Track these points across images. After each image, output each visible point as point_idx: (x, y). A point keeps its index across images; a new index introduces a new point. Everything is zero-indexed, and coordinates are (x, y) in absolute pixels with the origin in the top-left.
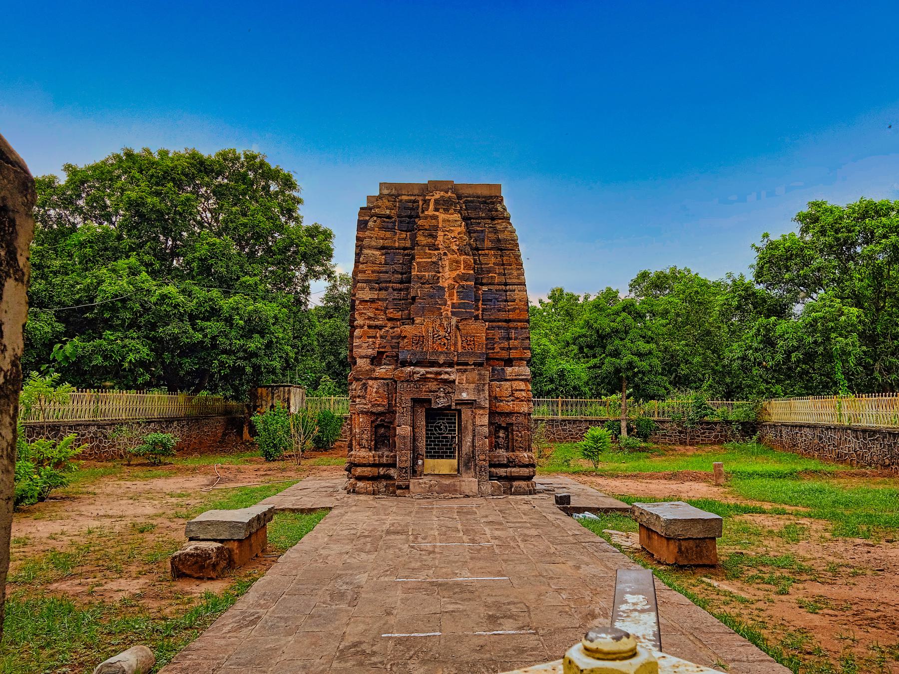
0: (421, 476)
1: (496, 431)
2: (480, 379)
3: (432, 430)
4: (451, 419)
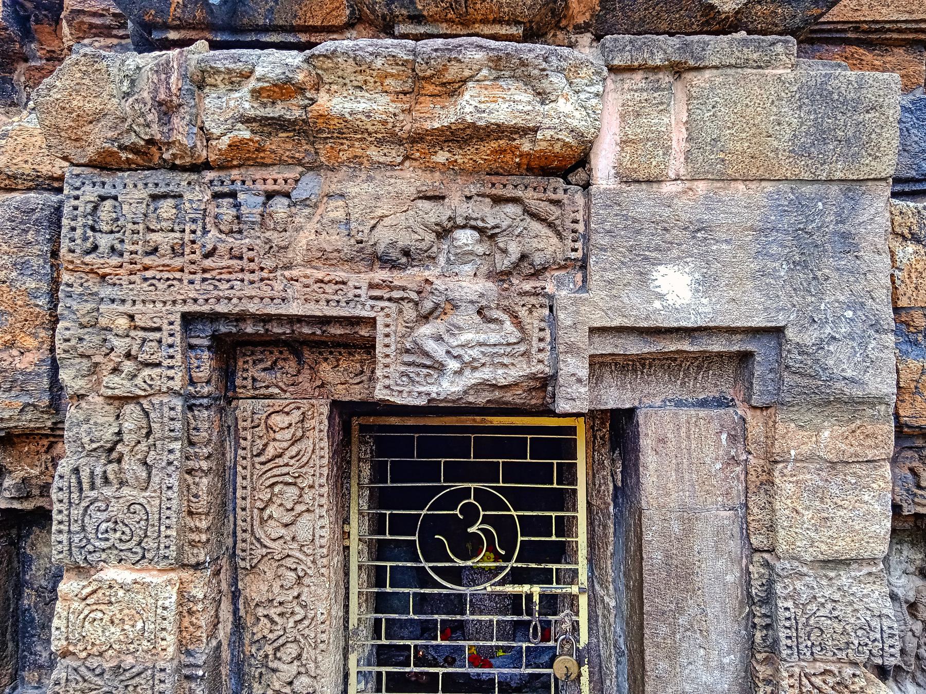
2: (822, 136)
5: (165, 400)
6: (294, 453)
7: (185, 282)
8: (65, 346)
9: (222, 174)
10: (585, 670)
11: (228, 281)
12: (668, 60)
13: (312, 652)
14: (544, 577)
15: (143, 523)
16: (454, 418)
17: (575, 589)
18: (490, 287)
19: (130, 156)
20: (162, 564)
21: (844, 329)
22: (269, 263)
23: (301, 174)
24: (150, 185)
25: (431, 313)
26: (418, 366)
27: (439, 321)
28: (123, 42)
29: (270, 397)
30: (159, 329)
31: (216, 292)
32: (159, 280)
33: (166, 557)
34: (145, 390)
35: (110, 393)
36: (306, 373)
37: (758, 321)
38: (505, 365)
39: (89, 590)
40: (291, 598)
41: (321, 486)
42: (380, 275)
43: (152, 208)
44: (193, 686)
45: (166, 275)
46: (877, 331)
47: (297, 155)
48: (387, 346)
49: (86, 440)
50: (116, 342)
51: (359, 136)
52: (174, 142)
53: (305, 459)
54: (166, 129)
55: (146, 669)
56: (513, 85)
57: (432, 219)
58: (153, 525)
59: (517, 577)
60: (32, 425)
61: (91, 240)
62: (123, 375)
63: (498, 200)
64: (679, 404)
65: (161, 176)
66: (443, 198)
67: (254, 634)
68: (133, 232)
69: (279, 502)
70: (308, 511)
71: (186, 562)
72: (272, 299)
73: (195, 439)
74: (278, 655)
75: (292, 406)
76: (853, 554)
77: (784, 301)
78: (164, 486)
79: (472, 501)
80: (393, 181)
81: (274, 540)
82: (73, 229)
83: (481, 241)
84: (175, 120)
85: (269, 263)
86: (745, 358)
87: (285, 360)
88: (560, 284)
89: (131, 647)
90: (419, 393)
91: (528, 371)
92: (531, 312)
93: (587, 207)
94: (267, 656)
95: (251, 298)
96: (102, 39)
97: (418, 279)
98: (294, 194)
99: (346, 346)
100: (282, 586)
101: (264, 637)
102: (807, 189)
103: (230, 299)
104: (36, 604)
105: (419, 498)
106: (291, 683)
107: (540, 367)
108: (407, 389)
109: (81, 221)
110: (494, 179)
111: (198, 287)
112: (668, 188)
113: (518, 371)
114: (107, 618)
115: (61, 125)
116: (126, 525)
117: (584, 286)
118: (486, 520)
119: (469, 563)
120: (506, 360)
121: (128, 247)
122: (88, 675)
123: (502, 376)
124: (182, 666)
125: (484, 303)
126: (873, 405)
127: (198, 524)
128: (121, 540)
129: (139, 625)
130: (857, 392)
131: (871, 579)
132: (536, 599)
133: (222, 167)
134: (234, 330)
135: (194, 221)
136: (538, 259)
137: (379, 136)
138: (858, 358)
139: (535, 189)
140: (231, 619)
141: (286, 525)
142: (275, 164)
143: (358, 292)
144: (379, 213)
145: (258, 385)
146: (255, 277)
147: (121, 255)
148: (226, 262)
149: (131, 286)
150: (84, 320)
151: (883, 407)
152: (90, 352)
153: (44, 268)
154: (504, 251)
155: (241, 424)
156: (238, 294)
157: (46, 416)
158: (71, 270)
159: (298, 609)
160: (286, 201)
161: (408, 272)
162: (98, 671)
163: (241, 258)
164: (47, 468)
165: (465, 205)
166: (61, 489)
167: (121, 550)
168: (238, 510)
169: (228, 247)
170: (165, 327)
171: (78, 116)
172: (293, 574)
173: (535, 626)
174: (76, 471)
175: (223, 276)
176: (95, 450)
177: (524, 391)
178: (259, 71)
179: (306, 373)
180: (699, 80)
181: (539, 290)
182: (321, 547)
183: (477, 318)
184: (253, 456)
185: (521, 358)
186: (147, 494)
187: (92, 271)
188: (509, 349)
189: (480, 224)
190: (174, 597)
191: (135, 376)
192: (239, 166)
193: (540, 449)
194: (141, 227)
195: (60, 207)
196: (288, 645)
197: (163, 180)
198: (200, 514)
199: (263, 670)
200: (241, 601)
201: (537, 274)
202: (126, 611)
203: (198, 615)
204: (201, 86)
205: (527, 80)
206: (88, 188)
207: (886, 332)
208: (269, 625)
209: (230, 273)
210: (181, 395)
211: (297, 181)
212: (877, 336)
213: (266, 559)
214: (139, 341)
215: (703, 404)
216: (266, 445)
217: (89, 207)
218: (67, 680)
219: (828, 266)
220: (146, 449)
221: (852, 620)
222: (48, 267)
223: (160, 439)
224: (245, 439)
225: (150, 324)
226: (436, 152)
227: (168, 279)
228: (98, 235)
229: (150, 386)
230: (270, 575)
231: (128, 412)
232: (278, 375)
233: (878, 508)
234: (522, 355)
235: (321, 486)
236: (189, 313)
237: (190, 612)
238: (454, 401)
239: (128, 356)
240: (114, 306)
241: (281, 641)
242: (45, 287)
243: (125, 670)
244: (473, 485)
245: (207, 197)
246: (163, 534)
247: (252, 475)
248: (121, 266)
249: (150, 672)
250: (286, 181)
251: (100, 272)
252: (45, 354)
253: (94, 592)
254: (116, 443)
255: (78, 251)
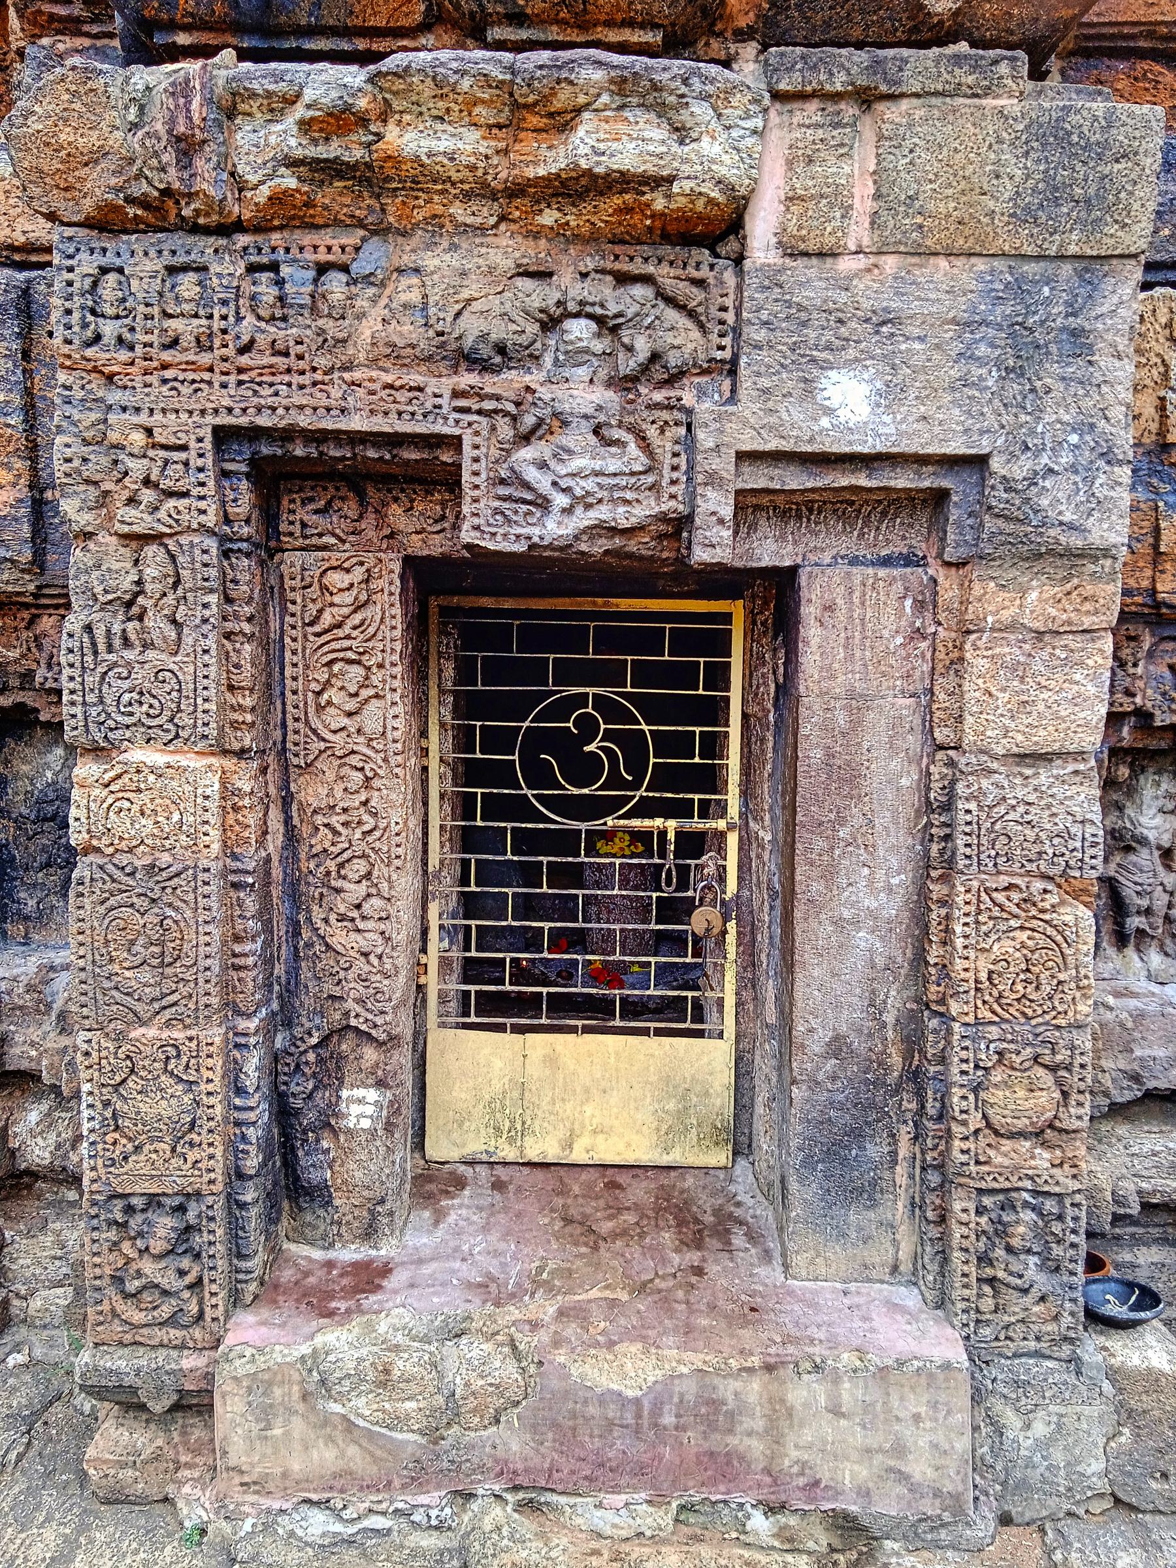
0: (369, 1233)
1: (1109, 784)
2: (1054, 193)
3: (502, 774)
4: (686, 675)
5: (196, 540)
6: (357, 622)
7: (216, 385)
8: (66, 467)
9: (260, 238)
10: (732, 926)
11: (271, 385)
12: (853, 84)
13: (385, 870)
14: (682, 810)
15: (174, 694)
16: (567, 600)
17: (721, 824)
18: (610, 398)
19: (139, 212)
20: (201, 746)
21: (1065, 459)
22: (322, 361)
23: (364, 240)
24: (165, 253)
25: (533, 431)
26: (516, 501)
27: (543, 442)
28: (99, 43)
29: (325, 548)
30: (184, 448)
31: (256, 400)
32: (182, 382)
33: (205, 737)
34: (170, 527)
35: (126, 529)
36: (371, 518)
37: (956, 447)
38: (627, 502)
39: (112, 774)
40: (357, 804)
41: (393, 665)
42: (467, 379)
43: (168, 285)
44: (242, 895)
45: (191, 376)
46: (1109, 462)
47: (358, 213)
48: (476, 474)
49: (98, 590)
50: (131, 463)
51: (440, 187)
52: (197, 193)
53: (371, 630)
54: (186, 175)
55: (186, 869)
56: (642, 116)
57: (536, 303)
58: (187, 697)
59: (645, 809)
60: (10, 588)
61: (92, 327)
62: (142, 507)
63: (623, 279)
64: (854, 561)
65: (178, 240)
66: (550, 275)
67: (311, 846)
68: (146, 318)
69: (339, 684)
70: (377, 696)
71: (227, 747)
72: (328, 410)
73: (233, 594)
74: (343, 872)
75: (354, 560)
76: (1056, 747)
77: (991, 421)
78: (199, 649)
79: (590, 710)
80: (483, 250)
81: (335, 732)
82: (69, 312)
83: (599, 335)
84: (199, 163)
85: (322, 361)
86: (940, 497)
87: (343, 499)
88: (702, 393)
89: (167, 843)
90: (518, 536)
91: (657, 509)
92: (662, 432)
93: (739, 288)
94: (328, 873)
95: (301, 408)
96: (67, 39)
97: (517, 385)
98: (354, 268)
99: (422, 481)
100: (345, 790)
101: (325, 850)
102: (1030, 268)
103: (274, 409)
104: (15, 838)
105: (518, 707)
106: (358, 907)
107: (673, 504)
108: (501, 531)
109: (78, 301)
110: (618, 249)
111: (232, 393)
112: (846, 264)
113: (645, 509)
114: (136, 808)
115: (46, 169)
116: (154, 697)
117: (733, 399)
118: (609, 736)
119: (586, 791)
120: (629, 495)
121: (140, 337)
122: (117, 874)
123: (623, 516)
124: (225, 872)
125: (602, 418)
126: (1095, 559)
127: (241, 701)
128: (148, 715)
129: (176, 817)
130: (1076, 541)
131: (1078, 779)
132: (671, 836)
133: (260, 228)
134: (279, 452)
135: (224, 302)
136: (673, 360)
137: (466, 187)
138: (1081, 497)
139: (671, 263)
140: (282, 830)
141: (350, 714)
142: (327, 226)
143: (438, 401)
144: (465, 294)
145: (309, 532)
146: (306, 379)
147: (132, 348)
148: (267, 360)
149: (146, 390)
150: (89, 435)
151: (1108, 562)
152: (98, 477)
153: (14, 373)
154: (630, 349)
155: (288, 583)
156: (285, 402)
157: (27, 577)
158: (69, 368)
159: (366, 817)
160: (343, 277)
161: (503, 376)
162: (128, 870)
163: (286, 354)
164: (29, 649)
165: (579, 285)
166: (71, 651)
167: (150, 727)
168: (288, 694)
169: (270, 339)
170: (193, 444)
171: (69, 155)
172: (360, 775)
173: (670, 869)
174: (88, 628)
175: (264, 378)
176: (110, 602)
177: (652, 539)
178: (309, 95)
179: (371, 518)
180: (893, 113)
181: (673, 402)
182: (395, 741)
183: (592, 439)
184: (305, 625)
185: (647, 493)
186: (178, 659)
187: (95, 370)
188: (633, 480)
189: (598, 311)
190: (217, 786)
191: (157, 509)
192: (281, 228)
193: (682, 642)
194: (156, 311)
195: (28, 288)
196: (355, 861)
197: (182, 246)
198: (242, 688)
199: (325, 890)
200: (294, 807)
201: (673, 379)
202: (158, 801)
203: (246, 812)
204: (231, 113)
205: (661, 110)
206: (83, 256)
207: (1120, 463)
208: (330, 836)
209: (273, 374)
210: (215, 534)
211: (357, 249)
212: (1107, 468)
213: (325, 755)
214: (160, 463)
215: (886, 562)
216: (320, 611)
217: (88, 281)
218: (92, 879)
219: (1051, 373)
220: (174, 602)
221: (1048, 826)
222: (19, 372)
223: (191, 590)
224: (294, 603)
225: (173, 440)
226: (541, 211)
227: (194, 381)
228: (100, 320)
229: (177, 521)
230: (330, 776)
231: (150, 554)
232: (335, 519)
233: (1092, 690)
234: (650, 489)
235: (393, 665)
236: (223, 426)
237: (236, 809)
238: (561, 549)
239: (147, 482)
240: (126, 416)
241: (346, 856)
242: (17, 400)
243: (161, 870)
244: (590, 690)
245: (240, 271)
246: (200, 709)
247: (304, 649)
248: (132, 363)
249: (191, 871)
250: (343, 248)
251: (106, 370)
252: (22, 491)
253: (119, 776)
254: (136, 595)
255: (76, 341)
